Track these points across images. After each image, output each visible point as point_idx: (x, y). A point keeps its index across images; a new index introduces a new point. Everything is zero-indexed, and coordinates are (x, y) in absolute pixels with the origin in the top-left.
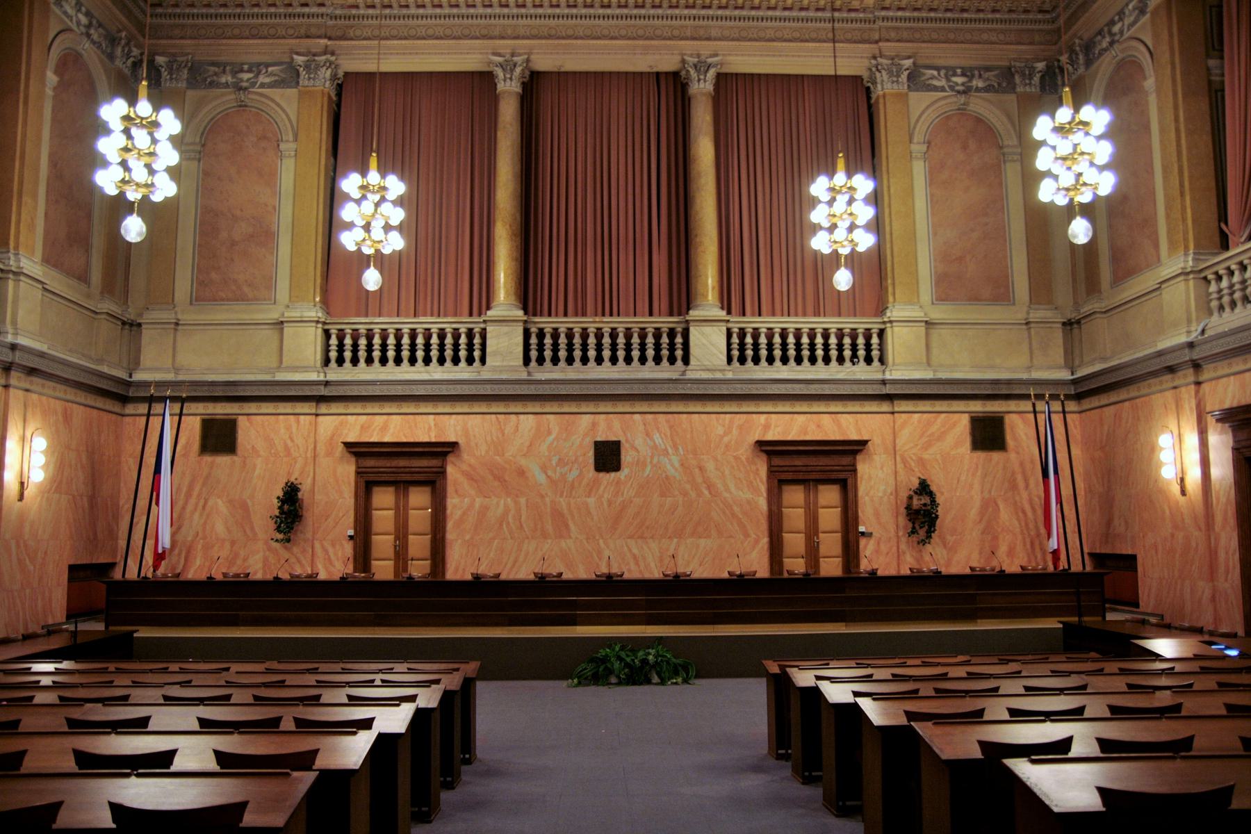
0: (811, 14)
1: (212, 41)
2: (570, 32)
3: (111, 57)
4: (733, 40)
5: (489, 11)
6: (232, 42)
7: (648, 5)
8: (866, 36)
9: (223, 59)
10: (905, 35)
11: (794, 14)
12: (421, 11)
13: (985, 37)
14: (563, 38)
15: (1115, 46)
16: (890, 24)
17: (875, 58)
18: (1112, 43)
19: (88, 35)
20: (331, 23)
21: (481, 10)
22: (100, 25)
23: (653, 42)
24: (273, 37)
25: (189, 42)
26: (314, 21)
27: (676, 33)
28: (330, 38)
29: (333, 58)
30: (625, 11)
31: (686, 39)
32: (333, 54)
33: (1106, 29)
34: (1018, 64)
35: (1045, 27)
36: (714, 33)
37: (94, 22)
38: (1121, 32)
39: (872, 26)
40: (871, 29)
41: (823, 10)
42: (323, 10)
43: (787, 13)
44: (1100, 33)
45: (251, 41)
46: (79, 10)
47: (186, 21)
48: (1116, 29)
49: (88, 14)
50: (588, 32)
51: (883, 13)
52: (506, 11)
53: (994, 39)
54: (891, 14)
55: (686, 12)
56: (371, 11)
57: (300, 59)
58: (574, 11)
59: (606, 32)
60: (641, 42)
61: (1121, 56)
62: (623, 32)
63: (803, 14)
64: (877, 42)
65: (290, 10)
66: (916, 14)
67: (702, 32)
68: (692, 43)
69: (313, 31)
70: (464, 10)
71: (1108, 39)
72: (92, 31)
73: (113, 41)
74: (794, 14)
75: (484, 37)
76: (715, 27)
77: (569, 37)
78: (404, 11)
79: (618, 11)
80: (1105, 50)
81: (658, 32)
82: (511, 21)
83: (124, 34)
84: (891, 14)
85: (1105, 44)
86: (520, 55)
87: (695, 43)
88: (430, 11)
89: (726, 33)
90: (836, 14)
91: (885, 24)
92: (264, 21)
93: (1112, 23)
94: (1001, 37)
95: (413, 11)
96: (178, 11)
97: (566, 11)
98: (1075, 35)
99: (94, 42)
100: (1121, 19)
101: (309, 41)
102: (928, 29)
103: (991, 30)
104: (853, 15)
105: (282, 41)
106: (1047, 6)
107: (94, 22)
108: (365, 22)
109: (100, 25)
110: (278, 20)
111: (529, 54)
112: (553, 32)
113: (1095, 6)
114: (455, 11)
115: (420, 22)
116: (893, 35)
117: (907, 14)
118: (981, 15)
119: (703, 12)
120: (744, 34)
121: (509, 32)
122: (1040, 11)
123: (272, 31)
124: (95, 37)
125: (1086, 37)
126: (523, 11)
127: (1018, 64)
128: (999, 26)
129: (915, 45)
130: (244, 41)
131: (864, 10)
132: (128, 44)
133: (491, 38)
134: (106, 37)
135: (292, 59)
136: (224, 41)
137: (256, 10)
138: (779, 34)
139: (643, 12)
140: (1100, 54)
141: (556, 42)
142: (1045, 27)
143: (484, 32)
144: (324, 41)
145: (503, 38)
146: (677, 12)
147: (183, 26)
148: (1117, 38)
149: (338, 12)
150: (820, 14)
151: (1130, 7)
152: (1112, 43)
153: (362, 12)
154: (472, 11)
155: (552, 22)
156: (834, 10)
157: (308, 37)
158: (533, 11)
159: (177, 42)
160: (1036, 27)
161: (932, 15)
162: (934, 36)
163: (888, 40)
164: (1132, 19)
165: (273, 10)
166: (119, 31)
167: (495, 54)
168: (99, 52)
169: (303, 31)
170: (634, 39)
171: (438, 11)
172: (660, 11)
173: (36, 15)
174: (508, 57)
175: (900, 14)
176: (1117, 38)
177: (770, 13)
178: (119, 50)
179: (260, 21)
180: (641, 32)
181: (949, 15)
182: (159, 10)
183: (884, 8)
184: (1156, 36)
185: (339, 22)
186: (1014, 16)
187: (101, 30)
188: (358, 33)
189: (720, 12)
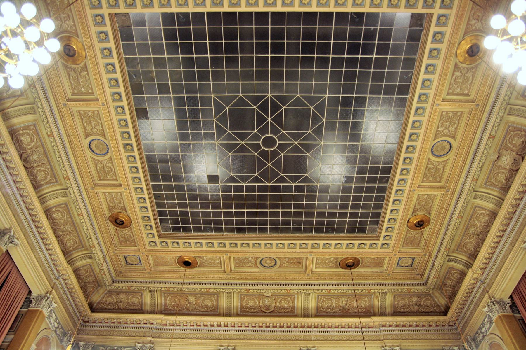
0: (353, 329)
1: (105, 337)
2: (253, 337)
3: (61, 341)
4: (321, 340)
5: (220, 328)
6: (113, 337)
7: (285, 326)
8: (378, 338)
9: (106, 344)
10: (394, 337)
11: (346, 329)
12: (192, 328)
13: (429, 337)
14: (250, 340)
15: (485, 337)
16: (387, 332)
17: (383, 347)
18: (484, 336)
19: (55, 331)
20: (154, 331)
21: (216, 328)
22: (62, 328)
23: (287, 342)
24: (130, 336)
25: (95, 337)
26: (148, 330)
27: (297, 338)
28: (153, 337)
29: (153, 346)
30: (276, 329)
31: (302, 340)
32: (153, 344)
33: (479, 331)
34: (446, 348)
35: (453, 332)
36: (313, 338)
37: (60, 326)
38: (486, 332)
39: (379, 333)
40: (380, 335)
41: (358, 327)
42: (152, 326)
43: (343, 329)
44: (477, 333)
45: (120, 337)
46: (56, 321)
47: (97, 329)
48: (483, 330)
49: (59, 323)
50: (260, 337)
51: (383, 328)
52: (226, 328)
53: (433, 338)
54: (387, 328)
55: (301, 329)
56: (171, 327)
57: (139, 345)
58: (255, 329)
59: (268, 337)
60: (282, 342)
61: (489, 342)
62: (275, 338)
63: (350, 329)
64: (383, 340)
65: (139, 325)
66: (397, 328)
67: (308, 337)
68: (304, 342)
69: (147, 334)
70: (209, 328)
71: (481, 335)
72: (58, 330)
73: (64, 334)
74: (346, 329)
75: (216, 339)
76: (313, 336)
77: (252, 339)
78: (185, 327)
79: (273, 329)
80: (482, 340)
81: (290, 338)
82: (228, 333)
83: (70, 332)
84: (387, 328)
85: (481, 338)
86: (231, 346)
87: (305, 342)
88: (195, 328)
89: (318, 338)
90: (364, 329)
91: (385, 332)
92: (128, 329)
93: (480, 328)
94: (436, 337)
95: (189, 327)
96: (95, 324)
97: (251, 329)
98: (467, 335)
99: (56, 334)
100: (483, 327)
101: (144, 338)
102: (404, 334)
103: (430, 334)
104: (371, 329)
105: (133, 338)
106: (451, 324)
107: (60, 326)
108: (169, 331)
109: (62, 328)
110: (134, 329)
111: (235, 346)
112: (245, 337)
113: (471, 322)
114: (206, 328)
115: (191, 332)
116: (389, 337)
117: (394, 328)
118: (425, 328)
119: (308, 329)
120: (326, 338)
121: (227, 337)
122: (449, 326)
123: (130, 334)
124: (58, 332)
125: (472, 335)
126: (234, 328)
127: (446, 348)
128: (433, 332)
129: (400, 341)
130: (117, 337)
131: (375, 327)
132: (70, 336)
133: (220, 339)
134: (62, 332)
135: (136, 345)
136: (110, 337)
137: (125, 325)
138: (341, 338)
139: (283, 329)
140: (481, 342)
141: (247, 341)
142: (453, 332)
143: (217, 337)
144: (151, 338)
145: (225, 339)
146: (297, 329)
147: (95, 330)
148: (485, 334)
149: (158, 327)
150: (357, 329)
151: (486, 321)
152: (484, 336)
153: (168, 327)
154: (213, 328)
155: (245, 333)
156: (362, 327)
157: (144, 336)
158: (237, 329)
159: (91, 336)
160: (449, 332)
161: (404, 328)
162: (407, 337)
163: (387, 339)
164: (488, 326)
165: (132, 325)
166: (69, 331)
167: (220, 346)
168: (57, 338)
169: (142, 334)
170: (280, 340)
171: (199, 328)
172: (290, 329)
173: (39, 320)
174: (226, 347)
175: (390, 328)
176: (485, 334)
177: (336, 329)
178: (66, 338)
179: (126, 329)
180: (282, 338)
181: (411, 328)
182: (87, 324)
183: (383, 326)
184: (501, 331)
185: (158, 331)
186: (439, 328)
187: (61, 330)
188: (165, 336)
189: (315, 329)
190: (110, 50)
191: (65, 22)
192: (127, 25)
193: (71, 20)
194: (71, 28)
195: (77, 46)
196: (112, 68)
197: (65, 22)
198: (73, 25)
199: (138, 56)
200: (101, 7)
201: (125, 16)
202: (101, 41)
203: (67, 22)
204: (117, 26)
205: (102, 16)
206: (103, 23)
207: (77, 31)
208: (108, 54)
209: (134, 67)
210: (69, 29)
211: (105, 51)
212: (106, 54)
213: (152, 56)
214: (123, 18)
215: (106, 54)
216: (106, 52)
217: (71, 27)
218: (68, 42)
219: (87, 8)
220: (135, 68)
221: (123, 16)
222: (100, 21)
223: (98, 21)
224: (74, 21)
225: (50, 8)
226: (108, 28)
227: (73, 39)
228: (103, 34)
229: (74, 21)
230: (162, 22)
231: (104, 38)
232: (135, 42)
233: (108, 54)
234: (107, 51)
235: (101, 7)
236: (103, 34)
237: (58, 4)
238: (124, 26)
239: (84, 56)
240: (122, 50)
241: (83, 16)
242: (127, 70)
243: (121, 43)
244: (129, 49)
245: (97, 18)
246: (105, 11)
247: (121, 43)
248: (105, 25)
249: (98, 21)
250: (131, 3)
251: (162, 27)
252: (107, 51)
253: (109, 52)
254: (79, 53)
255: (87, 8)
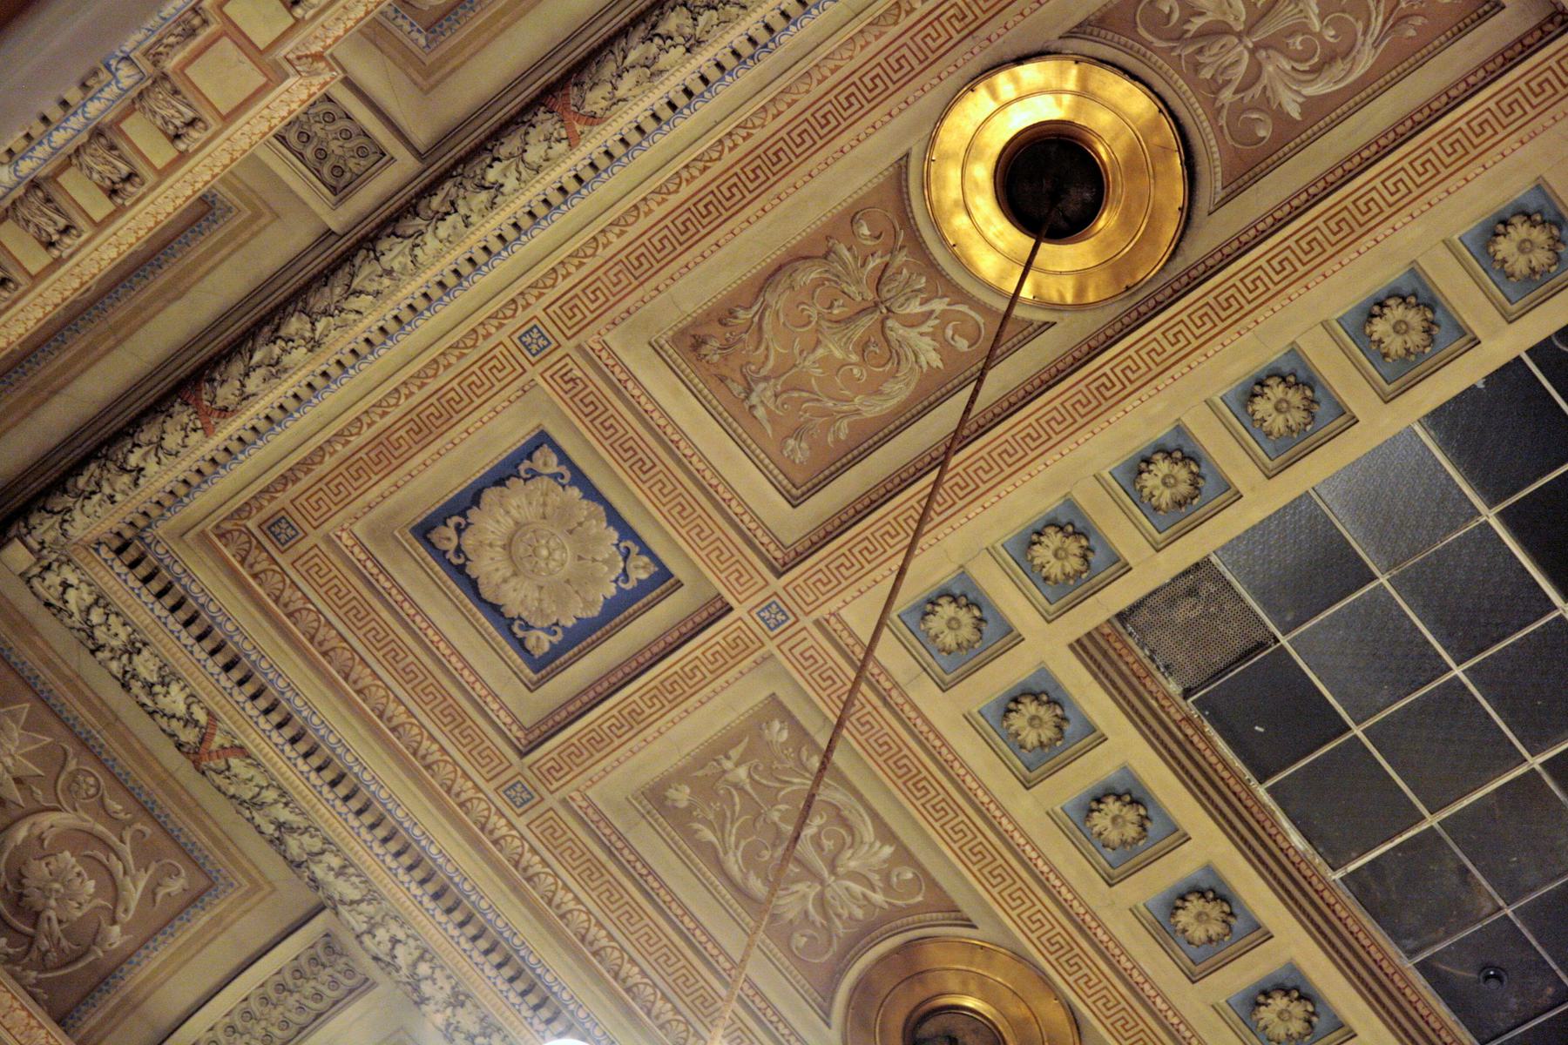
190: (1212, 890)
191: (833, 868)
192: (1239, 645)
193: (868, 831)
194: (888, 888)
195: (986, 994)
196: (1298, 1009)
197: (833, 868)
198: (892, 861)
199: (1432, 821)
200: (1010, 637)
201: (1192, 592)
202: (1120, 863)
203: (851, 862)
204: (1174, 688)
205: (1040, 692)
206: (1071, 735)
207: (934, 885)
208: (1216, 929)
209: (1455, 912)
210: (878, 898)
211: (1183, 918)
212: (1198, 933)
213: (1536, 762)
214: (1185, 611)
215: (1198, 933)
216: (1196, 920)
217: (886, 878)
218: (919, 993)
219: (925, 696)
220: (1467, 918)
221: (1172, 602)
222: (1048, 733)
223: (1031, 737)
224: (886, 834)
225: (708, 835)
226: (1125, 749)
227: (934, 956)
228: (1112, 806)
229: (886, 834)
230: (1469, 476)
231: (1131, 831)
232: (1357, 731)
233: (1216, 929)
234: (1195, 904)
235: (1010, 637)
236: (1112, 806)
237: (742, 772)
238: (1218, 659)
239: (1067, 1028)
240: (1297, 840)
241: (925, 767)
242: (1408, 965)
243: (1261, 792)
244: (1340, 805)
245: (1018, 721)
246: (1046, 645)
247: (1261, 792)
248: (1093, 735)
249: (1031, 737)
250: (1184, 489)
251: (1490, 516)
252: (1195, 904)
253: (1214, 910)
254: (1018, 1025)
255: (925, 696)
